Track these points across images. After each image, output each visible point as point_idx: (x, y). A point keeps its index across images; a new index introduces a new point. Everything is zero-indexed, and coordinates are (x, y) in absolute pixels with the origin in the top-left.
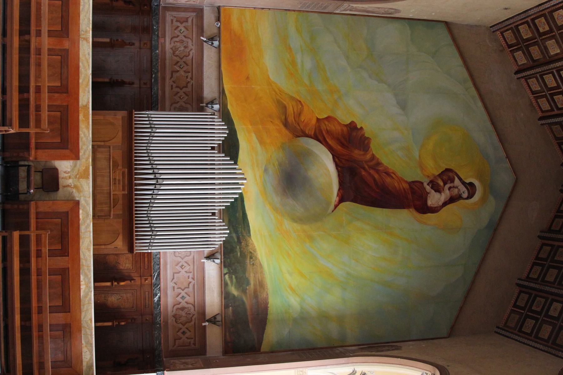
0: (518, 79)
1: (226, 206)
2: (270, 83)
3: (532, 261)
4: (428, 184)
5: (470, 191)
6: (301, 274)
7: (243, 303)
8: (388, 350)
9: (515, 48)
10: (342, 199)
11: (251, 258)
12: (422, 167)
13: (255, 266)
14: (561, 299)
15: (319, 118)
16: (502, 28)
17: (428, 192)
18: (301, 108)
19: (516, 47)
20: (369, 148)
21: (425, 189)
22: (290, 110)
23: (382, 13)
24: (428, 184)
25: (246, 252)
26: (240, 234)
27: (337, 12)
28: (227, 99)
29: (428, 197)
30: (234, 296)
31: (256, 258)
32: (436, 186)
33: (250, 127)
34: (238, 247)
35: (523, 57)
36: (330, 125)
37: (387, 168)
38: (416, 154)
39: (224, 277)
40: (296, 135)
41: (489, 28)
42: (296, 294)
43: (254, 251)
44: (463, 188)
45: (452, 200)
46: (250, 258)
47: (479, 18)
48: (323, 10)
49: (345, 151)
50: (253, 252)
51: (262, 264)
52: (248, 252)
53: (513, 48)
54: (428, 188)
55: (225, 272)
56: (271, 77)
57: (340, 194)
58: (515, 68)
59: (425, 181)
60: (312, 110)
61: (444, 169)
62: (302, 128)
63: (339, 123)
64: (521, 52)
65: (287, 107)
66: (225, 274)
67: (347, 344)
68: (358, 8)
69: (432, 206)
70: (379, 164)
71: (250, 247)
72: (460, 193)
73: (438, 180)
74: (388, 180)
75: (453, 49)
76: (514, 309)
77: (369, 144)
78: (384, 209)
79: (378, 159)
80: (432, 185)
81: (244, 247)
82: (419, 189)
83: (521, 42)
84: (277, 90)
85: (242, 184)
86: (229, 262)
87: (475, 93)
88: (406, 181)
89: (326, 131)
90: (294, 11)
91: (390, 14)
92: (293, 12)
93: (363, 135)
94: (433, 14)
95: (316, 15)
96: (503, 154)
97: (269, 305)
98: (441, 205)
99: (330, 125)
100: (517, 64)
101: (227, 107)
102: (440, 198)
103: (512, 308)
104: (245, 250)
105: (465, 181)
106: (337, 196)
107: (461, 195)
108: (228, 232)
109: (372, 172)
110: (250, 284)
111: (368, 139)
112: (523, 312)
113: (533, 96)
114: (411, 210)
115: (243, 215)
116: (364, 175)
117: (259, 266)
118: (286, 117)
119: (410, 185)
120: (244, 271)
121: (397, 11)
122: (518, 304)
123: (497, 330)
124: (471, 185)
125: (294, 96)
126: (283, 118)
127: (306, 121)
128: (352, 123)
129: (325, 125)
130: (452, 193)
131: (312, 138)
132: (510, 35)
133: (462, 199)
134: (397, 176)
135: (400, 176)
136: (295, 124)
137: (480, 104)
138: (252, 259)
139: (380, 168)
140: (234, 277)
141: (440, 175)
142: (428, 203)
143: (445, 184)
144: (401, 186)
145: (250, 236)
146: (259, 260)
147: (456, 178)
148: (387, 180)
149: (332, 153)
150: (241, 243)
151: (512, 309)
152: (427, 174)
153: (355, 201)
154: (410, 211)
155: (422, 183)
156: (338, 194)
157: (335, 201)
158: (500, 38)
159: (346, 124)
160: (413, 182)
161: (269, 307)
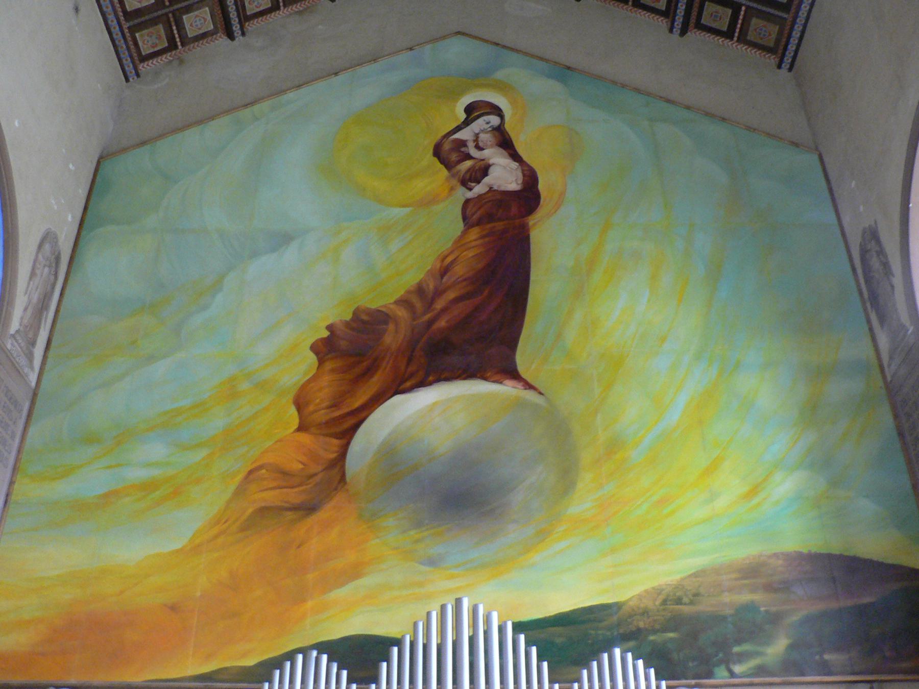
0: (243, 34)
1: (540, 659)
2: (194, 549)
3: (631, 10)
4: (470, 189)
5: (482, 112)
6: (711, 470)
7: (808, 620)
8: (881, 252)
9: (175, 32)
10: (512, 373)
11: (679, 601)
12: (427, 202)
13: (702, 590)
14: (696, 5)
15: (296, 427)
16: (128, 48)
17: (488, 189)
18: (267, 470)
19: (174, 28)
20: (379, 311)
21: (480, 197)
22: (271, 497)
23: (52, 278)
24: (470, 189)
25: (663, 616)
26: (615, 633)
27: (33, 378)
28: (226, 669)
29: (499, 189)
30: (792, 647)
31: (679, 586)
32: (474, 174)
33: (309, 604)
34: (652, 638)
35: (196, 13)
36: (318, 401)
37: (430, 273)
38: (398, 212)
39: (741, 677)
40: (339, 482)
41: (129, 84)
42: (765, 480)
43: (659, 594)
44: (479, 124)
45: (505, 143)
46: (681, 604)
47: (99, 85)
48: (22, 410)
49: (384, 364)
50: (661, 597)
51: (693, 571)
52: (664, 610)
53: (177, 36)
54: (479, 189)
55: (726, 674)
56: (177, 545)
57: (497, 377)
58: (222, 41)
59: (463, 196)
60: (277, 442)
61: (436, 159)
62: (320, 468)
63: (314, 378)
64: (184, 17)
65: (263, 504)
66: (732, 674)
67: (871, 353)
68: (25, 321)
69: (520, 181)
70: (420, 290)
71: (648, 603)
72: (490, 129)
73: (458, 172)
74: (460, 270)
75: (163, 146)
76: (736, 35)
77: (369, 312)
78: (533, 277)
79: (408, 292)
80: (471, 182)
81: (651, 619)
82: (480, 208)
83: (164, 11)
84: (215, 531)
85: (474, 611)
86: (695, 663)
87: (265, 106)
88: (462, 233)
89: (333, 409)
90: (12, 483)
91: (58, 259)
92: (16, 486)
93: (347, 324)
94: (71, 166)
95: (32, 430)
96: (404, 57)
97: (805, 551)
98: (517, 164)
99: (318, 401)
100: (212, 35)
101: (250, 667)
102: (500, 165)
103: (735, 39)
104: (655, 618)
105: (463, 120)
106: (501, 383)
107: (495, 127)
108: (617, 652)
109: (439, 305)
110: (753, 602)
111: (356, 313)
112: (743, 8)
113: (282, 8)
114: (531, 223)
115: (557, 626)
116: (447, 322)
117: (700, 579)
118: (290, 509)
119: (472, 226)
120: (717, 619)
121: (48, 238)
122: (725, 29)
123: (786, 65)
124: (469, 109)
125: (232, 487)
126: (290, 515)
127: (304, 459)
128: (314, 348)
129: (315, 411)
130: (489, 143)
131: (348, 443)
132: (146, 37)
133: (504, 125)
134: (452, 252)
135: (449, 245)
136: (310, 486)
137: (291, 95)
138: (682, 598)
139: (431, 287)
140: (736, 649)
141: (448, 165)
142: (516, 190)
143: (468, 157)
144: (474, 244)
145: (618, 606)
146: (683, 579)
147: (457, 136)
148: (461, 273)
149: (390, 395)
150: (639, 630)
151: (737, 41)
152: (447, 191)
153: (512, 343)
154: (535, 224)
155: (467, 201)
156: (494, 382)
157: (513, 387)
158: (153, 66)
159: (317, 366)
160: (465, 218)
161: (810, 551)
